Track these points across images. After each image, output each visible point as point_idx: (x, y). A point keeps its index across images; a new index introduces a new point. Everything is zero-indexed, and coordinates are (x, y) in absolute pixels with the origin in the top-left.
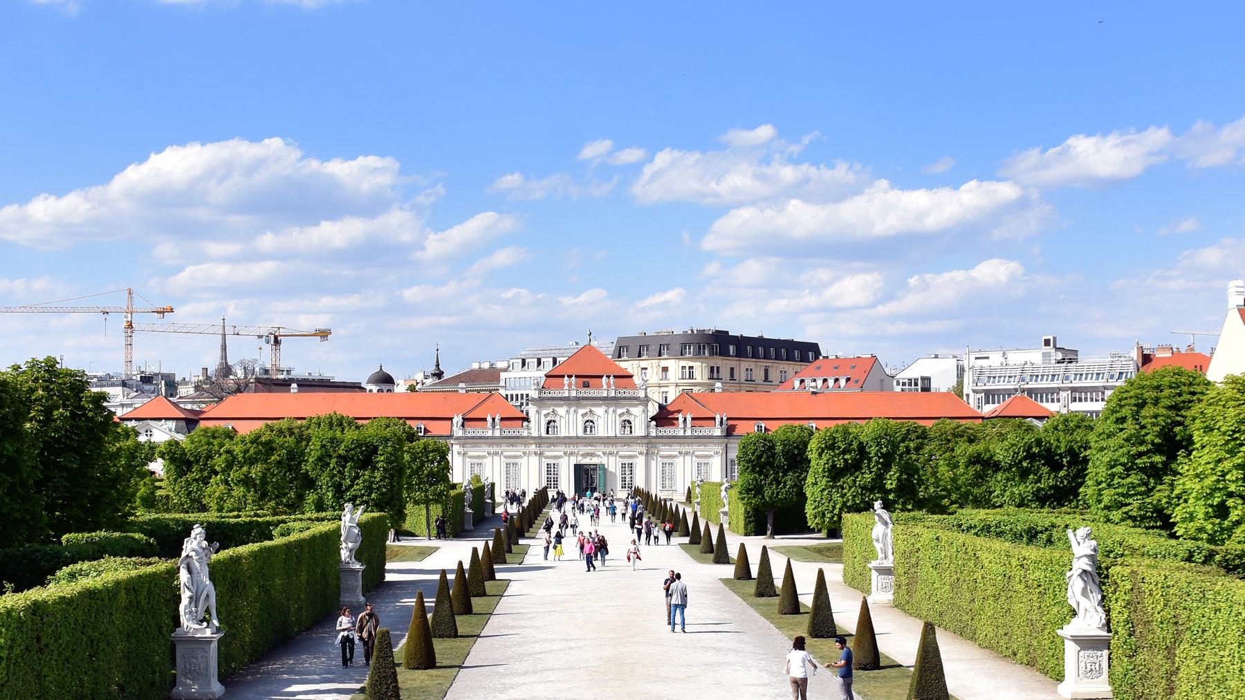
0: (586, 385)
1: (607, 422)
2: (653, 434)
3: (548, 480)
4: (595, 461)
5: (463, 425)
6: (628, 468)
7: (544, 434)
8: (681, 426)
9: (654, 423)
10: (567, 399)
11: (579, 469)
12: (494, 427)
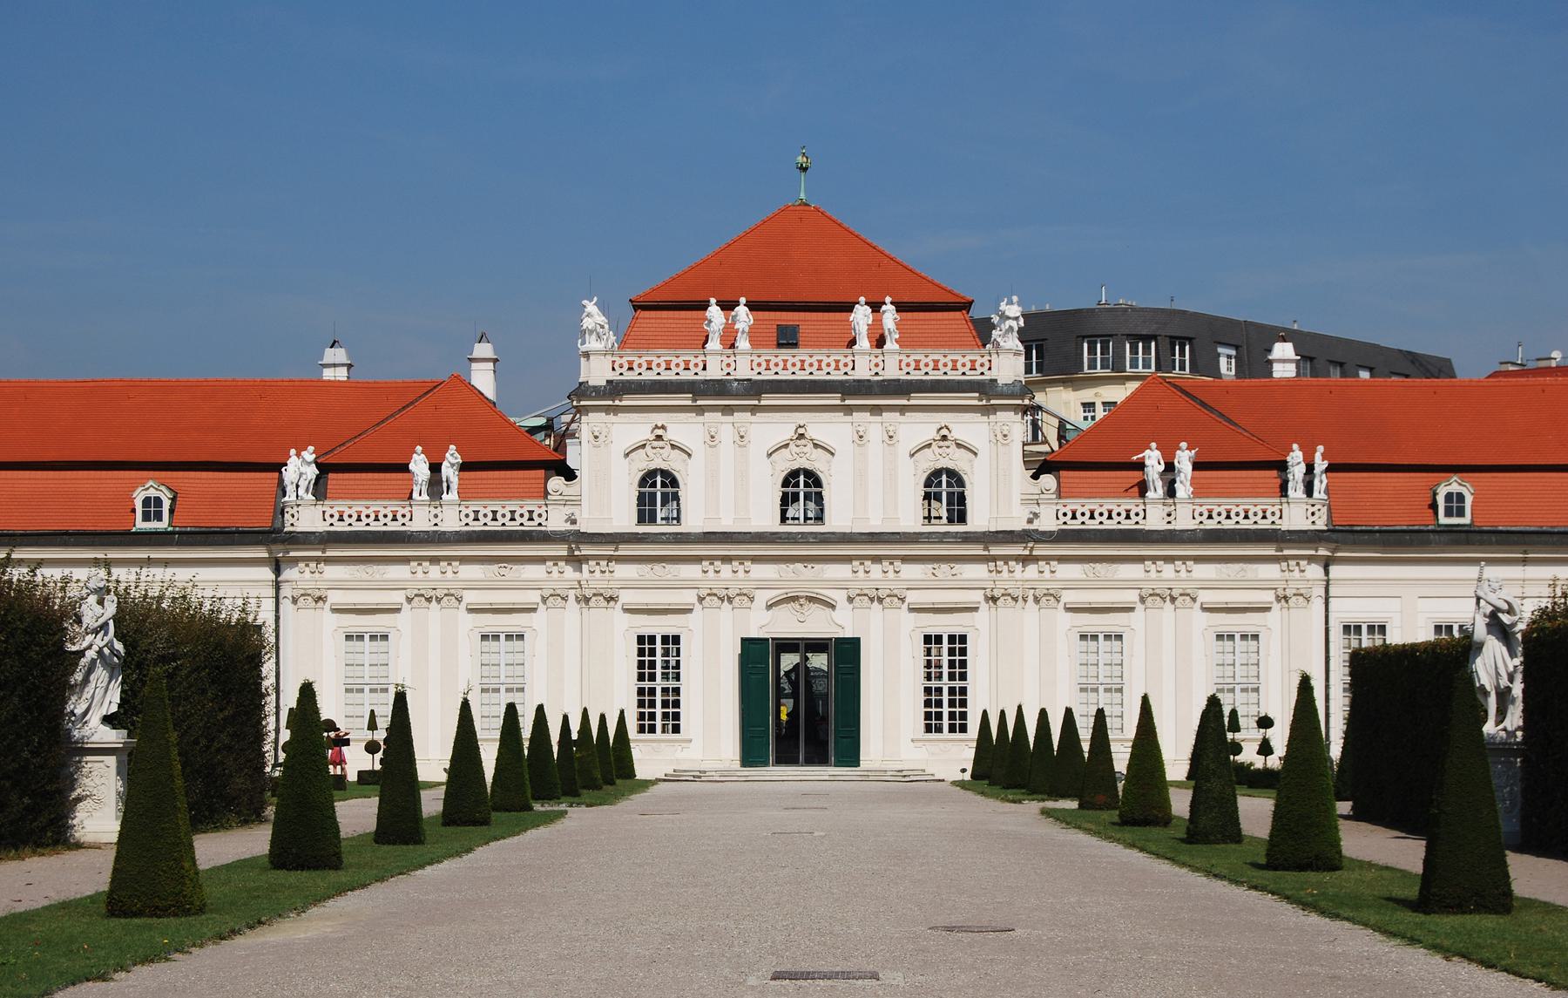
0: (787, 339)
1: (873, 472)
2: (1047, 523)
3: (645, 697)
4: (816, 624)
5: (320, 490)
6: (948, 658)
7: (624, 518)
8: (1157, 491)
9: (1048, 480)
10: (718, 388)
11: (755, 654)
12: (436, 486)
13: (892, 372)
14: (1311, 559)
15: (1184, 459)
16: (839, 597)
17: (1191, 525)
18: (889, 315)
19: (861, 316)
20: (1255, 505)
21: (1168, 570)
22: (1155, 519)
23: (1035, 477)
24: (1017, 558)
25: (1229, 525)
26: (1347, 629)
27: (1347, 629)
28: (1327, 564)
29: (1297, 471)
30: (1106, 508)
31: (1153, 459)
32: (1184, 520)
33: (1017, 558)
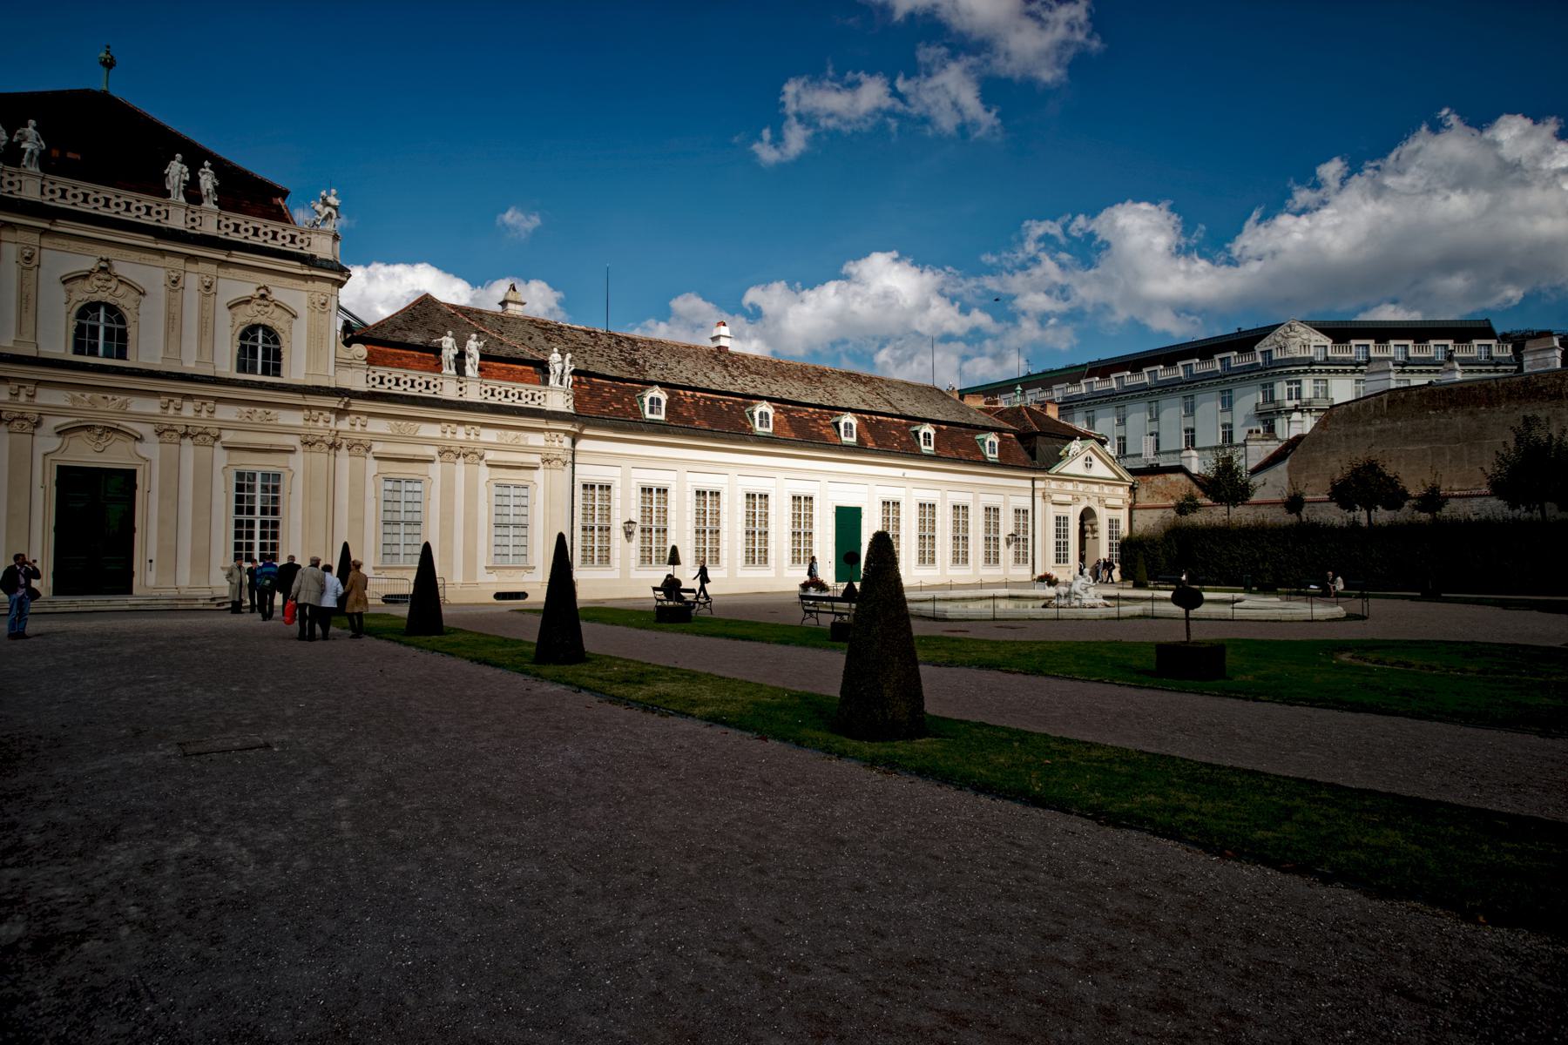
9: (360, 350)
13: (209, 227)
14: (567, 433)
15: (473, 347)
16: (146, 430)
17: (479, 399)
18: (207, 181)
19: (176, 171)
20: (527, 389)
21: (461, 433)
22: (450, 391)
23: (348, 343)
24: (332, 410)
25: (506, 402)
26: (585, 486)
27: (585, 486)
28: (575, 438)
29: (558, 368)
30: (409, 380)
31: (448, 345)
32: (473, 394)
33: (332, 410)
